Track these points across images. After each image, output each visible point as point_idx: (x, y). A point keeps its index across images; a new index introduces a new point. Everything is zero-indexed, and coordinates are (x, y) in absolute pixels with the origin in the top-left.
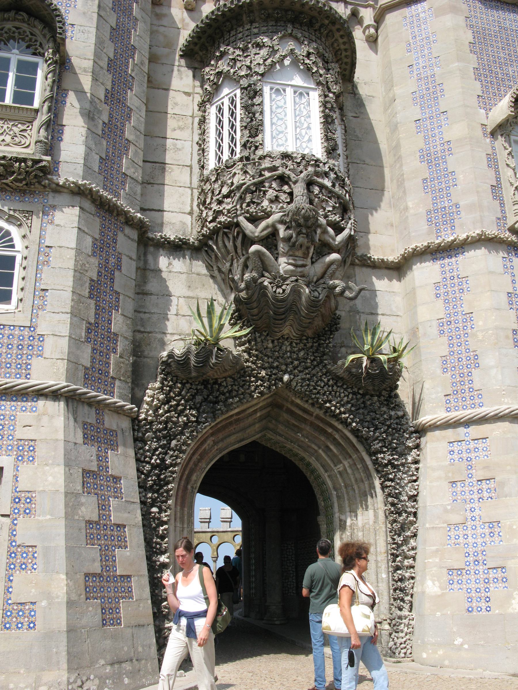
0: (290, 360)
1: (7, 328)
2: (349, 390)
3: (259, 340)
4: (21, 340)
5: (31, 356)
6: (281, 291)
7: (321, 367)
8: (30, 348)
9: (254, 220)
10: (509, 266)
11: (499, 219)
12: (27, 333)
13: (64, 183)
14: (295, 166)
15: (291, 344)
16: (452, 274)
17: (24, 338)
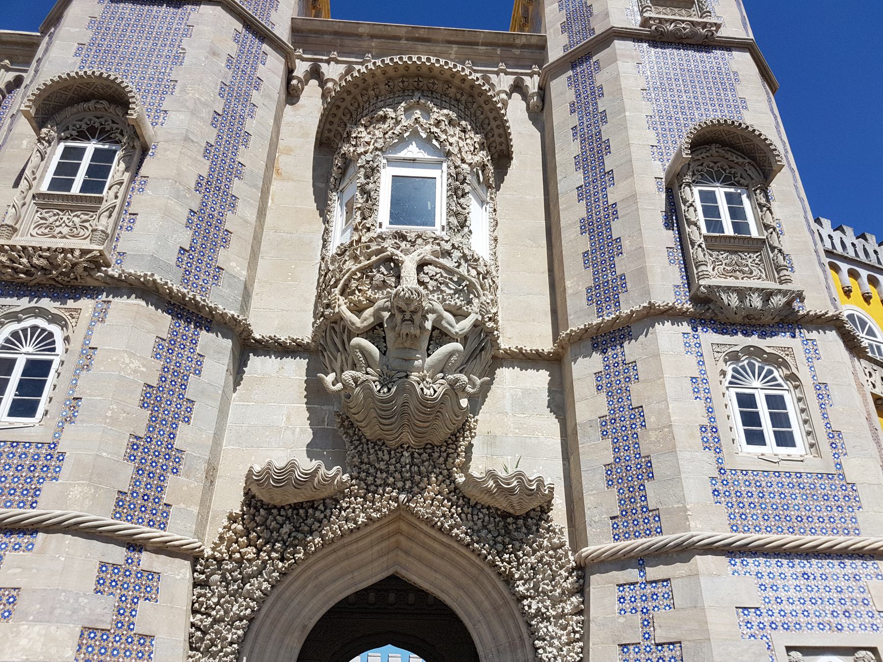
0: (408, 475)
1: (21, 445)
2: (485, 511)
3: (372, 451)
4: (35, 460)
5: (44, 479)
6: (386, 390)
7: (448, 482)
8: (45, 469)
9: (358, 310)
10: (692, 344)
11: (677, 286)
12: (44, 451)
13: (120, 275)
14: (408, 246)
15: (412, 454)
16: (617, 360)
17: (39, 457)
